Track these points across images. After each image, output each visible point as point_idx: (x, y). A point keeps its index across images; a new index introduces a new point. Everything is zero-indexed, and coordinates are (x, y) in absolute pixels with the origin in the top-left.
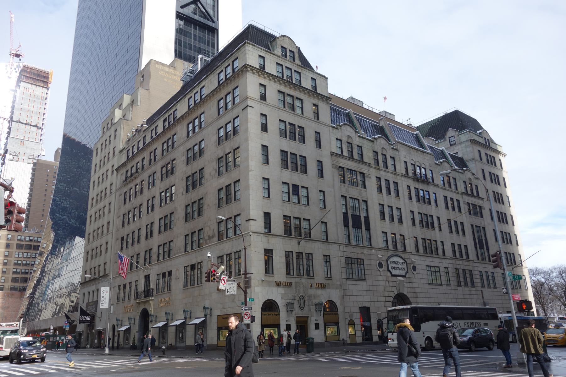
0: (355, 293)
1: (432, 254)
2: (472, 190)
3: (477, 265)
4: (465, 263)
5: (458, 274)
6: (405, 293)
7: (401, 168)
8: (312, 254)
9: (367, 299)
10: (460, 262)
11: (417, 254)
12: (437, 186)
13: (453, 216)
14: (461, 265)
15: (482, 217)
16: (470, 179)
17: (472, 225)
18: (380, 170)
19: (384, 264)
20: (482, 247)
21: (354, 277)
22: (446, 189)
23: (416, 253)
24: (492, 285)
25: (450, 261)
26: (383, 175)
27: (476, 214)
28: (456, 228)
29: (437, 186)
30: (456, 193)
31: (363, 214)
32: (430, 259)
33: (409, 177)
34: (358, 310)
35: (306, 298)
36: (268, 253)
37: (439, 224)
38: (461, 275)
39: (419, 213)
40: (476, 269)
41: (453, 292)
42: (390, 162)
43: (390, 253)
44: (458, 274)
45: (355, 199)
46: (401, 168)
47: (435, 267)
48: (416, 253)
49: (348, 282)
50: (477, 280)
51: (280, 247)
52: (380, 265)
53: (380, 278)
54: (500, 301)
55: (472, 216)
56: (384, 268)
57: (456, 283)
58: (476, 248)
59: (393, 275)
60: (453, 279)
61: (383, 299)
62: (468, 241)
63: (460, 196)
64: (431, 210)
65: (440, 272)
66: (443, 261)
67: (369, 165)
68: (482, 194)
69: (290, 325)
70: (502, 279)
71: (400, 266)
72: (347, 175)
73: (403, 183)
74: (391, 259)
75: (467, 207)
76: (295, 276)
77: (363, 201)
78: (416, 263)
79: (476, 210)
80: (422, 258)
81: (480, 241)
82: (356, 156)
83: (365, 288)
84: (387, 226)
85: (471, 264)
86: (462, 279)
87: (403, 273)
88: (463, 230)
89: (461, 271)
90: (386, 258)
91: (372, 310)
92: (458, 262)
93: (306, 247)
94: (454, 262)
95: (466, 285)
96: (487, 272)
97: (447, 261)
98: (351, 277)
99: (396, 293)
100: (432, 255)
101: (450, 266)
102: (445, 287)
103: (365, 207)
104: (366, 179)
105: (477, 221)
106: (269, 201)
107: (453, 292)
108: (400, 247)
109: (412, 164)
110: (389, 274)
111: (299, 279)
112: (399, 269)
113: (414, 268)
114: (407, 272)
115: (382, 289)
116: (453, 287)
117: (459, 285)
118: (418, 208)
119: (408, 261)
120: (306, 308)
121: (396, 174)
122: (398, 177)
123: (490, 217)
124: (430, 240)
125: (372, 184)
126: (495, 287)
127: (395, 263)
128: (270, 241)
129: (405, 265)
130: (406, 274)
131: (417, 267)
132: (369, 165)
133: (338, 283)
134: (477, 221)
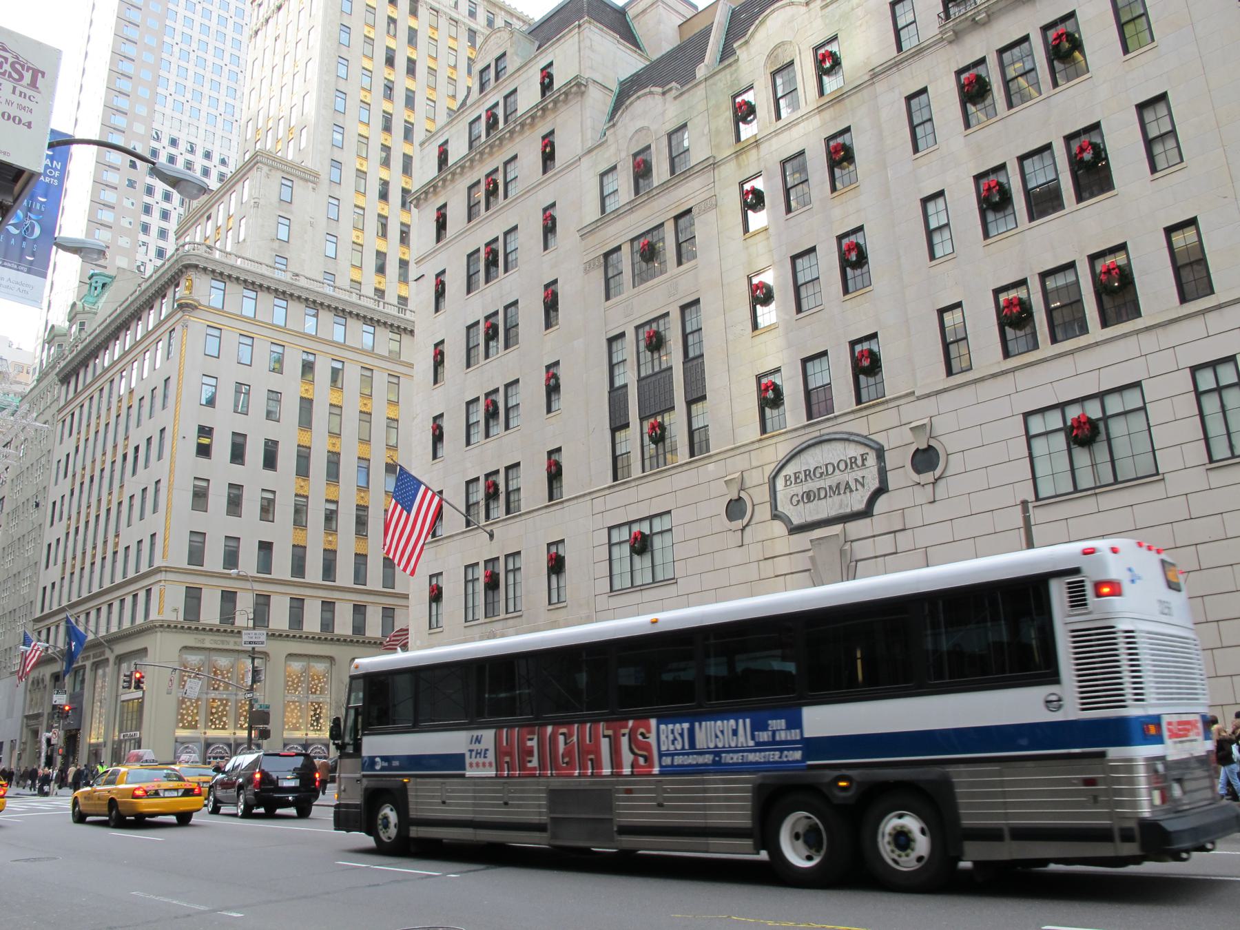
87: (857, 501)
114: (882, 490)
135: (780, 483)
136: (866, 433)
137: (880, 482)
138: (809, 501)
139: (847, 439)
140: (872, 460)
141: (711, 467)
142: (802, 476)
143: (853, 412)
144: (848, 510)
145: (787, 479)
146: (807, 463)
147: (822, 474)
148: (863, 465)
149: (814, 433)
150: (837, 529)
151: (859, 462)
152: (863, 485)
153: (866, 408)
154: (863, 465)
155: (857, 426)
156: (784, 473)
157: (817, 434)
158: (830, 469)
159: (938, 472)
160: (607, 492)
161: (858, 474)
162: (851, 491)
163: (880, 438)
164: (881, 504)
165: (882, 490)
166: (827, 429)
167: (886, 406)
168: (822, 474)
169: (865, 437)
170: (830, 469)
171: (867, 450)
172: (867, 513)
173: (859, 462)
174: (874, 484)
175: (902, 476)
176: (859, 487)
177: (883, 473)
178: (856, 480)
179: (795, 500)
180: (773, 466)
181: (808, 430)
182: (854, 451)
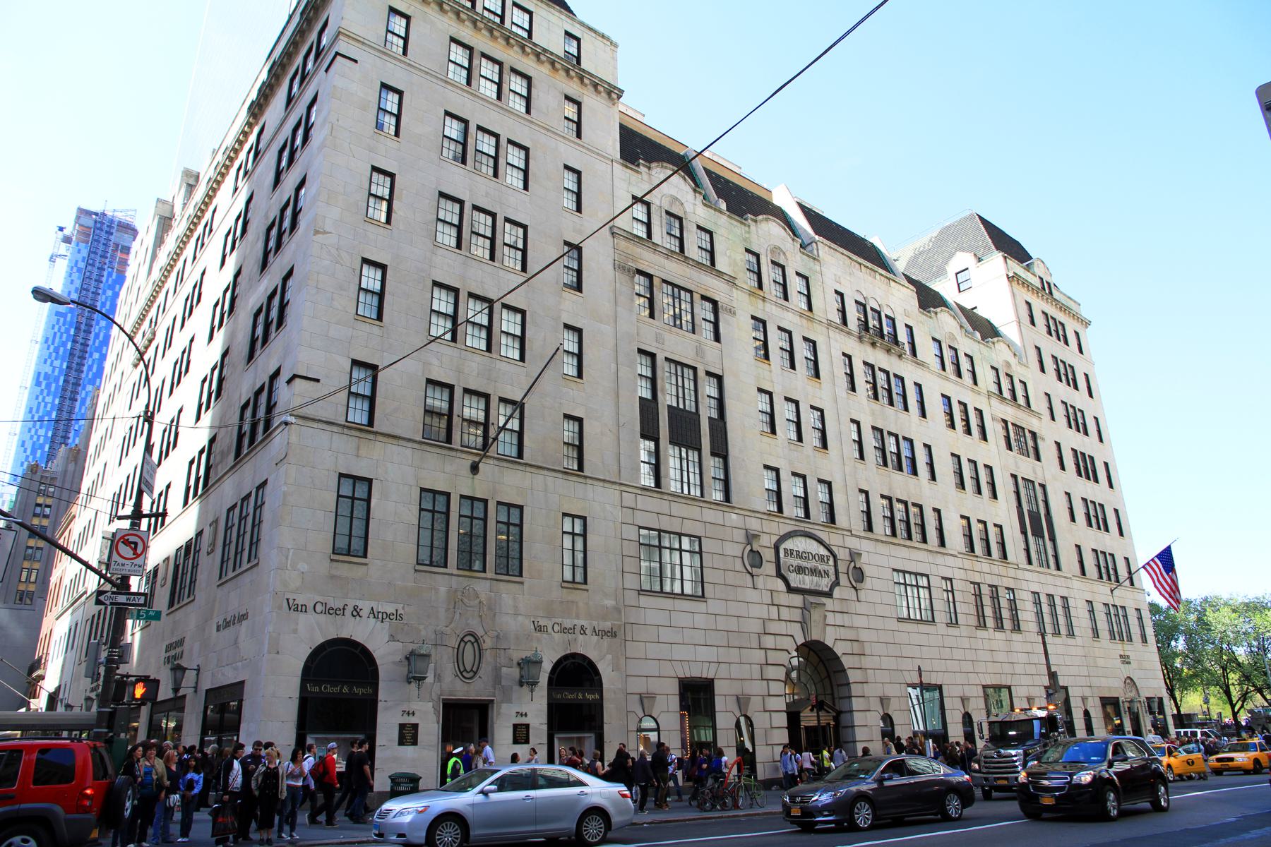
0: (666, 635)
1: (910, 538)
2: (1013, 391)
3: (1028, 575)
4: (995, 569)
5: (978, 596)
6: (829, 643)
7: (826, 306)
8: (521, 508)
9: (704, 654)
10: (985, 566)
11: (869, 535)
12: (922, 364)
13: (969, 447)
14: (987, 571)
15: (1038, 459)
16: (1008, 364)
17: (1014, 477)
18: (764, 299)
19: (768, 555)
20: (1038, 533)
21: (667, 588)
22: (947, 379)
23: (863, 534)
24: (1063, 630)
25: (958, 562)
26: (777, 316)
27: (1024, 452)
28: (971, 477)
29: (922, 364)
30: (973, 390)
31: (707, 412)
32: (904, 552)
33: (849, 333)
34: (674, 688)
35: (488, 643)
36: (356, 493)
37: (931, 465)
38: (987, 601)
39: (873, 428)
40: (1024, 585)
41: (965, 643)
42: (795, 284)
43: (785, 529)
44: (978, 596)
45: (683, 365)
46: (826, 306)
47: (916, 574)
48: (863, 534)
49: (645, 601)
50: (1027, 614)
51: (400, 476)
52: (756, 559)
53: (752, 595)
54: (1084, 671)
55: (1015, 453)
56: (769, 568)
57: (973, 621)
58: (1024, 532)
59: (790, 589)
60: (966, 609)
61: (759, 656)
62: (1003, 512)
63: (985, 400)
64: (907, 423)
65: (929, 588)
66: (940, 559)
67: (732, 281)
68: (1039, 404)
69: (415, 726)
70: (1087, 615)
71: (822, 567)
72: (663, 299)
73: (833, 346)
74: (789, 544)
75: (1000, 426)
76: (490, 574)
77: (709, 374)
78: (864, 559)
79: (1023, 441)
80: (882, 548)
81: (1035, 518)
82: (692, 251)
84: (780, 451)
85: (1011, 573)
86: (988, 611)
87: (824, 584)
88: (992, 484)
89: (985, 590)
90: (774, 539)
91: (719, 688)
92: (977, 566)
93: (501, 483)
94: (967, 563)
95: (1000, 626)
96: (1050, 596)
97: (950, 561)
98: (658, 588)
99: (800, 641)
100: (908, 543)
101: (956, 574)
102: (941, 628)
103: (714, 393)
104: (722, 316)
105: (1026, 467)
106: (376, 330)
107: (965, 643)
108: (818, 514)
109: (857, 302)
110: (780, 585)
111: (465, 582)
113: (859, 575)
114: (836, 583)
115: (756, 627)
116: (964, 631)
117: (982, 625)
118: (873, 414)
119: (842, 554)
120: (486, 670)
121: (811, 319)
122: (818, 327)
123: (1057, 461)
124: (905, 503)
125: (739, 330)
126: (1071, 634)
127: (799, 555)
128: (363, 452)
129: (831, 562)
130: (832, 589)
131: (868, 571)
132: (732, 281)
133: (610, 603)
134: (1026, 467)
155: (823, 535)
172: (829, 594)
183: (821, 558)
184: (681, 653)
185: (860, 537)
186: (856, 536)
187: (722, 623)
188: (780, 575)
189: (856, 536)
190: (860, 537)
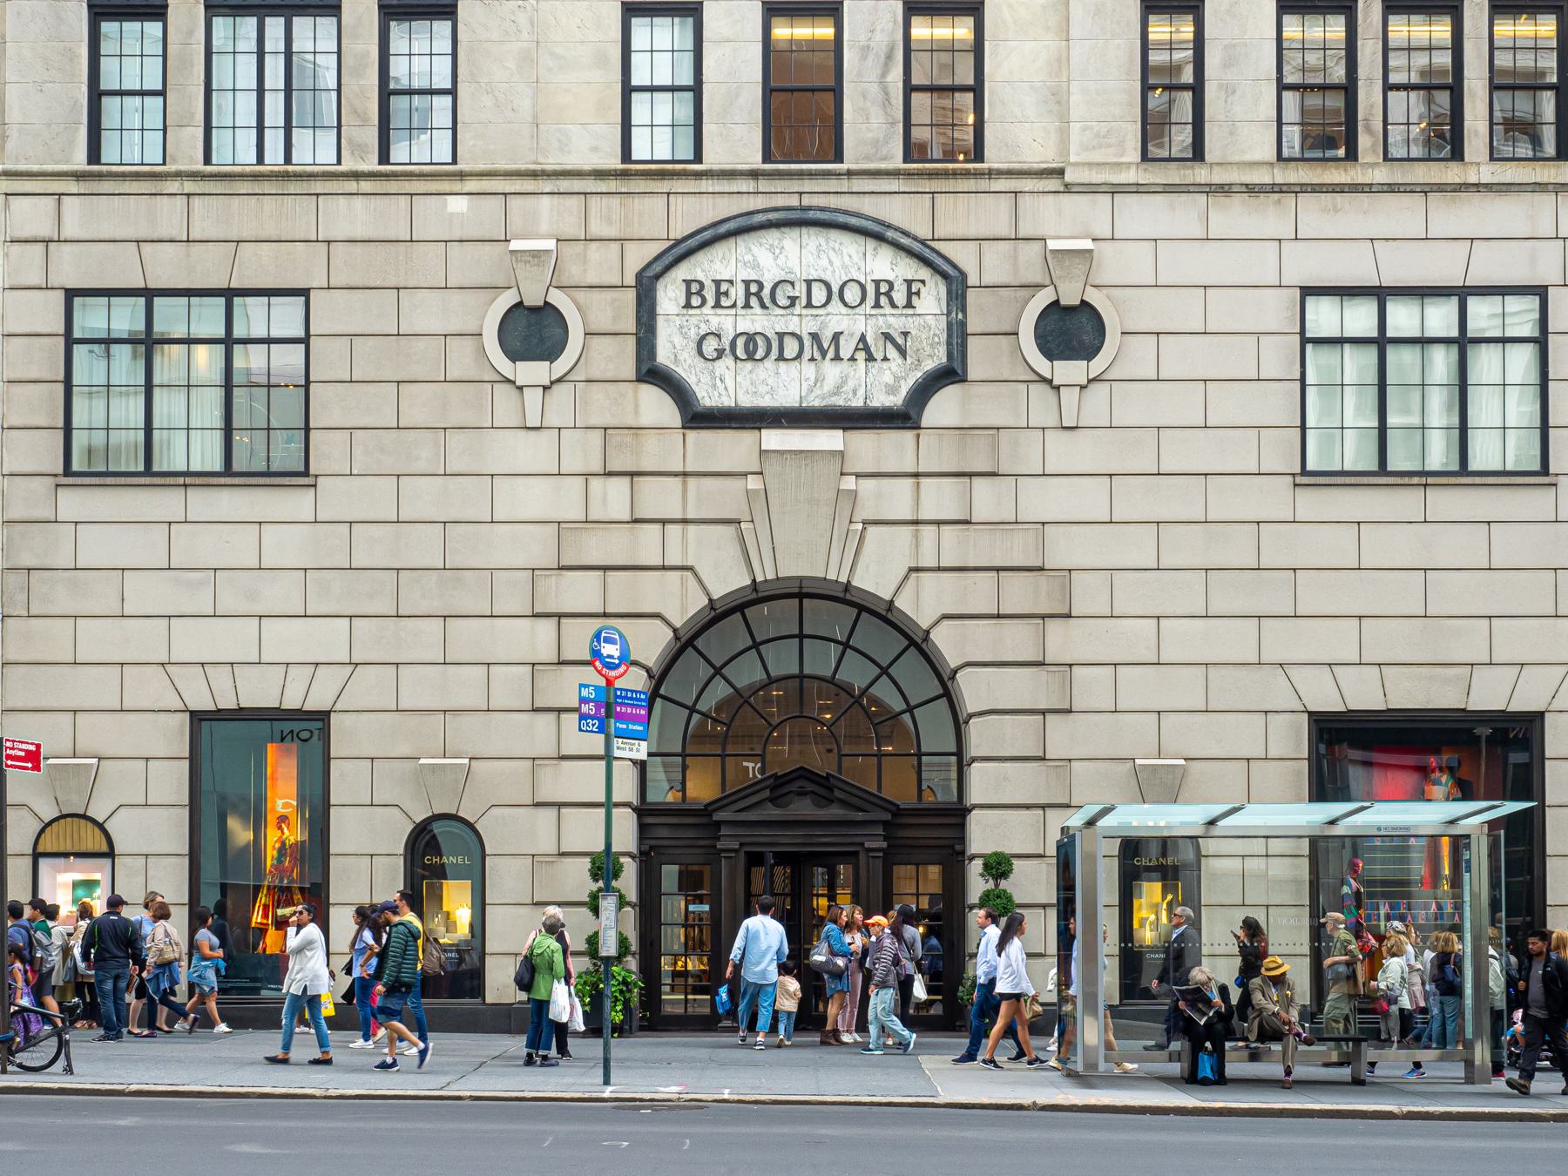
83: (284, 546)
87: (885, 385)
110: (656, 406)
112: (825, 348)
113: (1071, 330)
114: (950, 374)
135: (669, 296)
136: (923, 232)
137: (950, 355)
138: (750, 357)
139: (876, 233)
140: (933, 298)
141: (458, 205)
142: (738, 293)
143: (895, 174)
144: (857, 402)
145: (693, 290)
146: (756, 266)
147: (793, 300)
148: (909, 305)
149: (783, 195)
150: (830, 439)
151: (900, 296)
152: (903, 352)
153: (920, 174)
154: (909, 305)
155: (903, 210)
156: (682, 272)
157: (794, 201)
158: (819, 295)
159: (1098, 364)
160: (73, 187)
161: (894, 321)
162: (870, 358)
163: (962, 255)
164: (943, 408)
165: (950, 374)
166: (818, 194)
167: (983, 184)
168: (793, 300)
169: (923, 242)
170: (819, 295)
171: (924, 273)
172: (903, 418)
173: (900, 296)
174: (936, 358)
175: (1006, 350)
176: (892, 353)
177: (958, 336)
178: (887, 337)
179: (710, 347)
180: (655, 248)
181: (764, 185)
182: (884, 265)
183: (882, 292)
184: (191, 641)
185: (1115, 190)
186: (1091, 189)
187: (373, 547)
188: (652, 374)
189: (1091, 189)
190: (1115, 190)
